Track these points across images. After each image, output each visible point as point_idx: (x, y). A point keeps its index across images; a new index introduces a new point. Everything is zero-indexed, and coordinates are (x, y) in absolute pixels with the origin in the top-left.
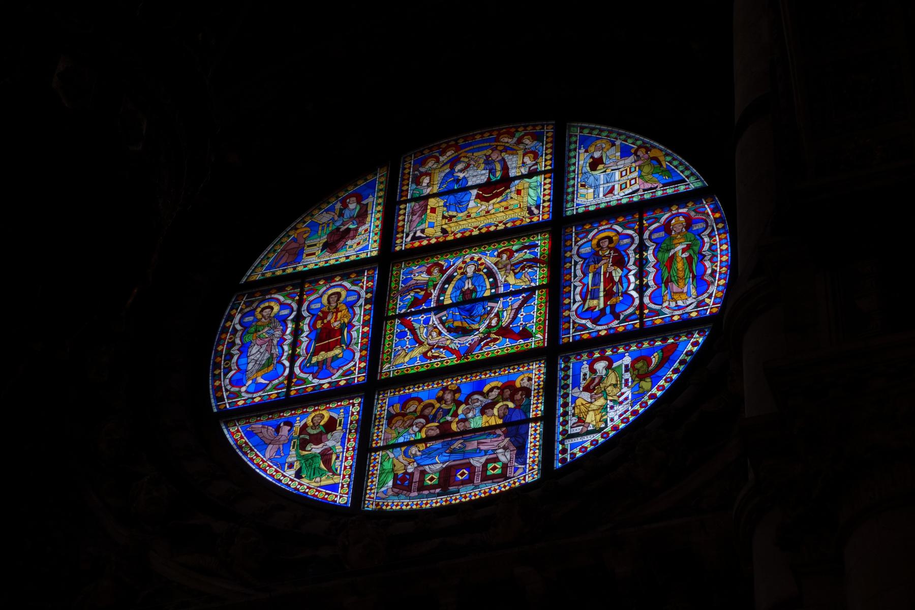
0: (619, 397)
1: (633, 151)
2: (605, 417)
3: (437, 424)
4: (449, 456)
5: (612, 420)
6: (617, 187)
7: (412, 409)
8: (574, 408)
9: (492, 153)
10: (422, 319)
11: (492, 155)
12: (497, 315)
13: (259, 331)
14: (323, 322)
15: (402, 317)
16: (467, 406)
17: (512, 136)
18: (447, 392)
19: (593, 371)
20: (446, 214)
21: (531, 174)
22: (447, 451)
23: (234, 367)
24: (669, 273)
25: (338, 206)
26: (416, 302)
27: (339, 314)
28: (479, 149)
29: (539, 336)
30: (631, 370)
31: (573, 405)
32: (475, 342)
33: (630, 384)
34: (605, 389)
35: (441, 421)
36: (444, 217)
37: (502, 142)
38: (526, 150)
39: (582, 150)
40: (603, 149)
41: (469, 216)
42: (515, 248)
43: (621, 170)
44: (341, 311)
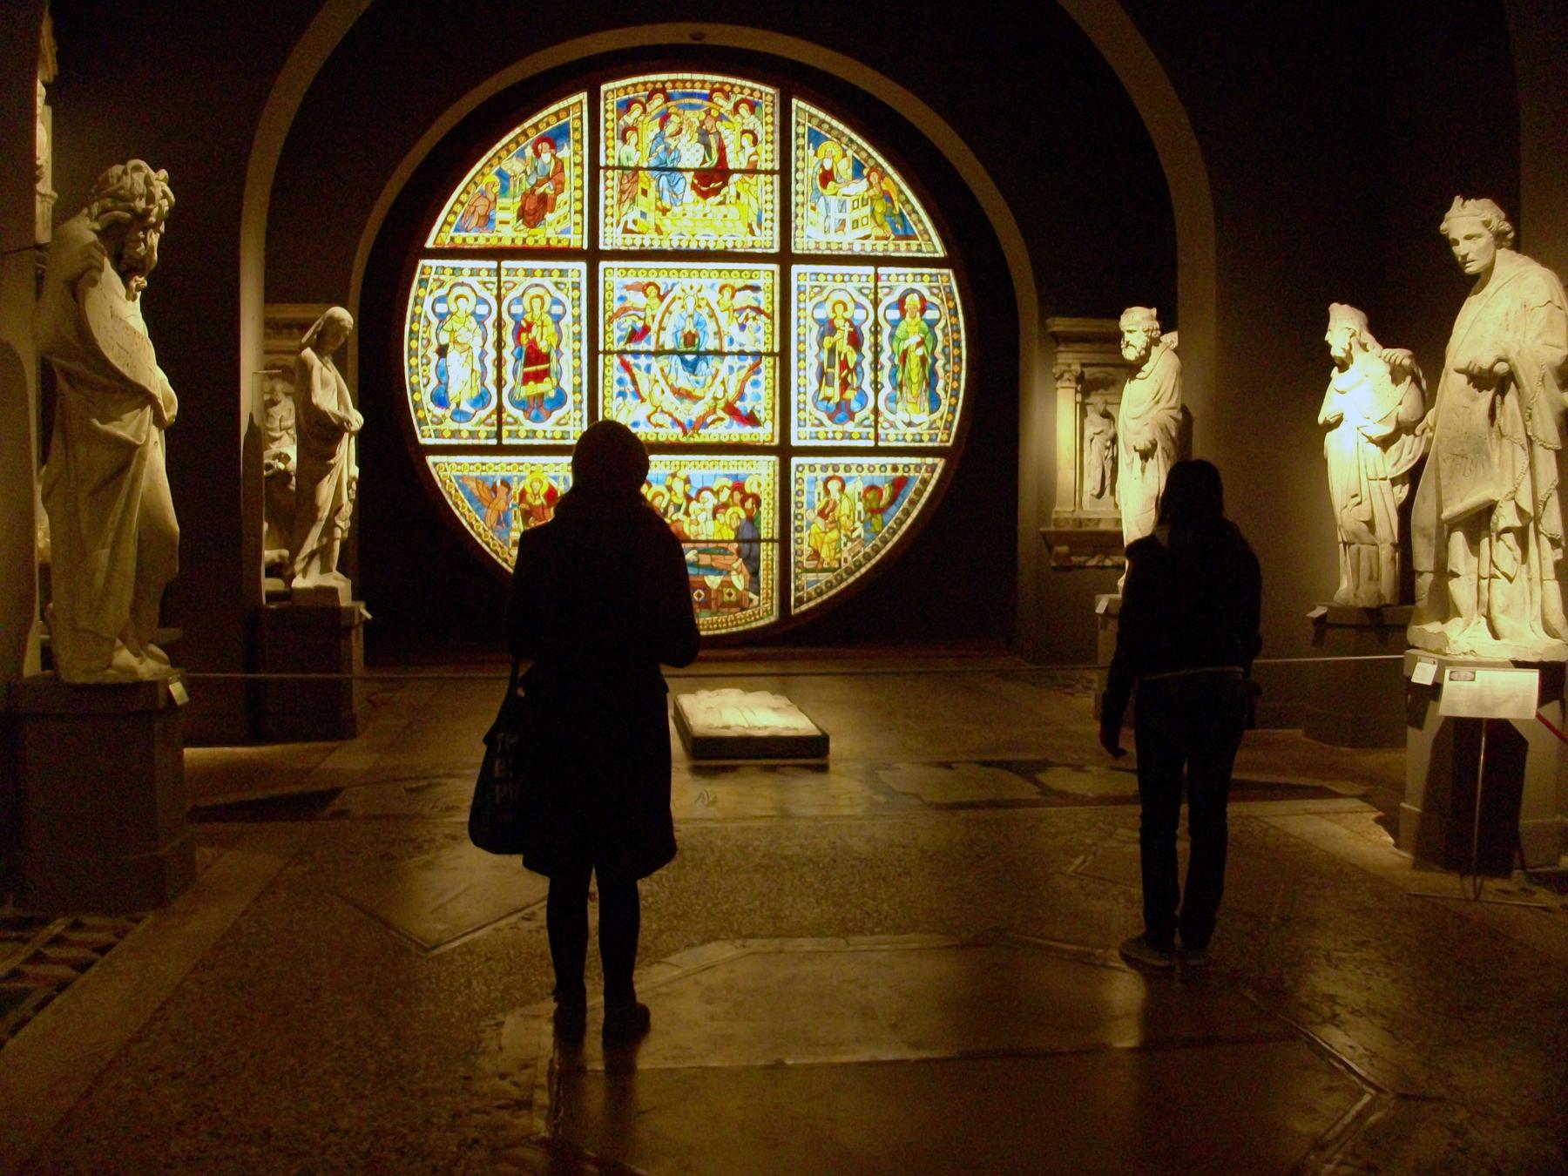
2: (838, 556)
5: (846, 561)
6: (849, 224)
12: (723, 382)
14: (527, 337)
15: (621, 353)
17: (727, 98)
19: (827, 492)
20: (659, 204)
21: (752, 171)
23: (433, 375)
24: (903, 372)
25: (529, 152)
26: (636, 335)
28: (692, 107)
29: (768, 425)
33: (862, 518)
36: (657, 208)
38: (746, 128)
39: (811, 152)
40: (833, 157)
42: (739, 283)
43: (853, 198)
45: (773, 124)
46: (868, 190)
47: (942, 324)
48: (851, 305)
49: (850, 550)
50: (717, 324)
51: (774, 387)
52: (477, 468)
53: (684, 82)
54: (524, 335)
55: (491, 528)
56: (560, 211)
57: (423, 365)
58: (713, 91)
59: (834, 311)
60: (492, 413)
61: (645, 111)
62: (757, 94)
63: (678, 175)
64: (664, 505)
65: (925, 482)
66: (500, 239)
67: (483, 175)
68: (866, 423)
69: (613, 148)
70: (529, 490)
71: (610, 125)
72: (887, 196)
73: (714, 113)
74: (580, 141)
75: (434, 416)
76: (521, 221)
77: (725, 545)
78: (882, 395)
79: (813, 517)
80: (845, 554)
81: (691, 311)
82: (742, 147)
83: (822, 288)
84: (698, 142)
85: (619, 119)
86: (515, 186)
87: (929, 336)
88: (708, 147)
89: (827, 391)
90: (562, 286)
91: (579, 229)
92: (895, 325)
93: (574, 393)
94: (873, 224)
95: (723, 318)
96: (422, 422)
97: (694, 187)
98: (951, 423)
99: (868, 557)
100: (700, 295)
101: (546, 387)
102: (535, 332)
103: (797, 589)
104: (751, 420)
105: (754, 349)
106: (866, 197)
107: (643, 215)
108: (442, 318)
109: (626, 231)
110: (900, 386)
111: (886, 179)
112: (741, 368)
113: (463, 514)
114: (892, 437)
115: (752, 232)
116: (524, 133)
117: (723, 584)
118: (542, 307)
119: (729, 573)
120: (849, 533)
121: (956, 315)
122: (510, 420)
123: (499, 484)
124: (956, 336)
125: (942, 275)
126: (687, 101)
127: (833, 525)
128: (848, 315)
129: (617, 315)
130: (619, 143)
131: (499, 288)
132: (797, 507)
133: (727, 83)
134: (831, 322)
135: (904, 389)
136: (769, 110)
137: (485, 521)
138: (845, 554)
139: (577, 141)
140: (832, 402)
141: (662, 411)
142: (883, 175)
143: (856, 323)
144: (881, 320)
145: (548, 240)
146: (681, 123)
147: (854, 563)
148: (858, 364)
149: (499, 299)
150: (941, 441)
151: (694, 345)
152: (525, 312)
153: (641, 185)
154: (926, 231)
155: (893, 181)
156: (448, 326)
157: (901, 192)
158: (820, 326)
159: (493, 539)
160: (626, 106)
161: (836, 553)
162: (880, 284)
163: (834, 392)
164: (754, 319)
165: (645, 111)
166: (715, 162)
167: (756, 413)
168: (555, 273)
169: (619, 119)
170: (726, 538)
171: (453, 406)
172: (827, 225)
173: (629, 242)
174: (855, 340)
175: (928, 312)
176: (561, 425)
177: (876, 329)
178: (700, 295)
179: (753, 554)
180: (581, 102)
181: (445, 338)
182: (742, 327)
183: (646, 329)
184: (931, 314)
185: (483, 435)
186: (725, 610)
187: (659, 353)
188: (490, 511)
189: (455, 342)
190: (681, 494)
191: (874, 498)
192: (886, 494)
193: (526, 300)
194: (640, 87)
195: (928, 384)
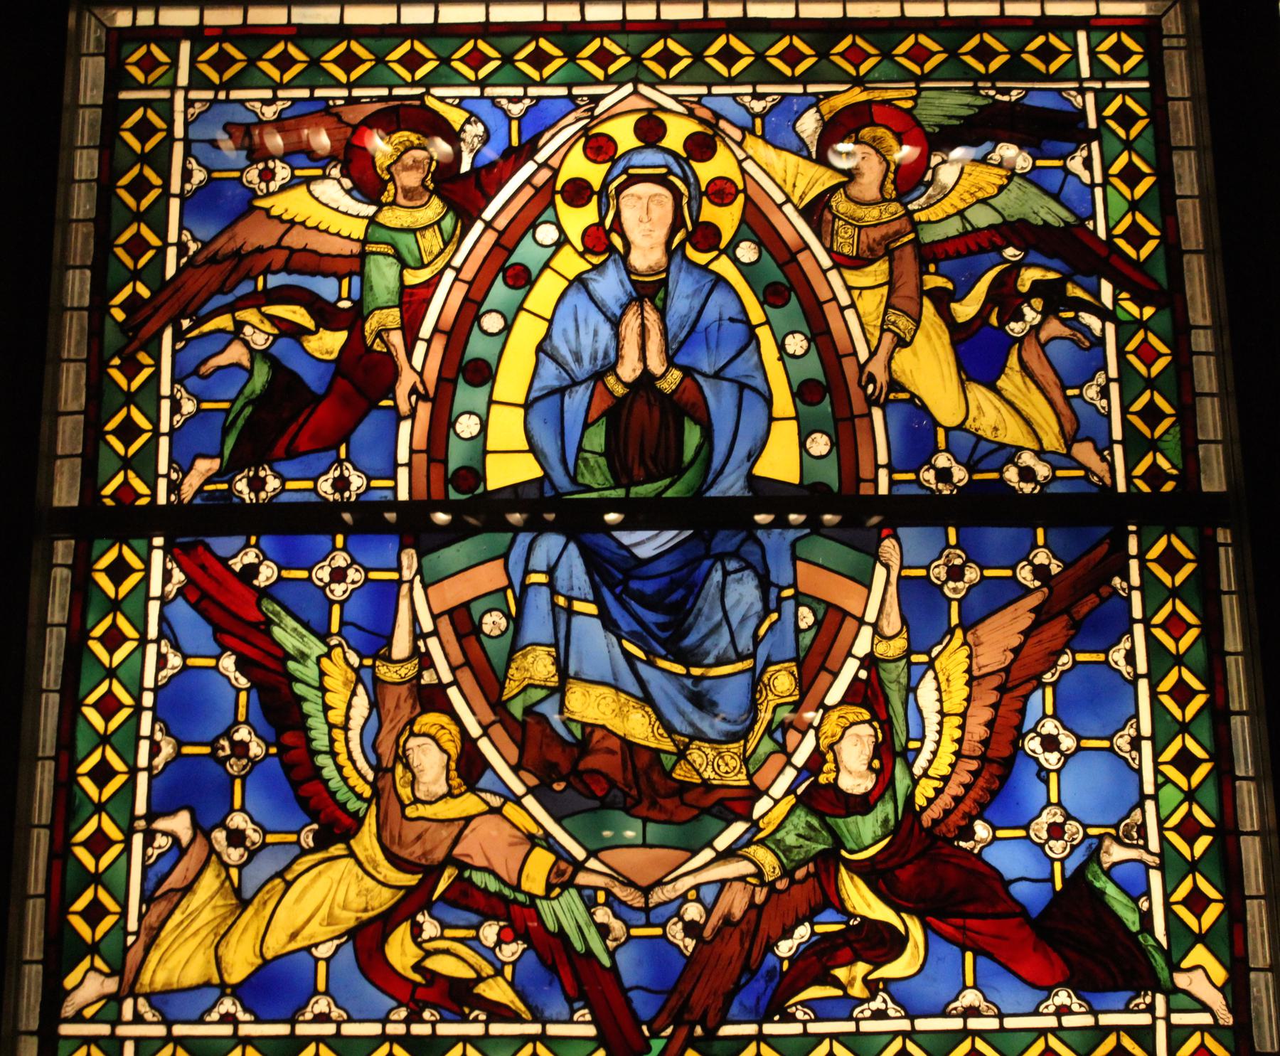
10: (338, 590)
32: (727, 920)
50: (819, 333)
100: (706, 171)
151: (676, 470)
164: (1052, 297)
178: (706, 171)
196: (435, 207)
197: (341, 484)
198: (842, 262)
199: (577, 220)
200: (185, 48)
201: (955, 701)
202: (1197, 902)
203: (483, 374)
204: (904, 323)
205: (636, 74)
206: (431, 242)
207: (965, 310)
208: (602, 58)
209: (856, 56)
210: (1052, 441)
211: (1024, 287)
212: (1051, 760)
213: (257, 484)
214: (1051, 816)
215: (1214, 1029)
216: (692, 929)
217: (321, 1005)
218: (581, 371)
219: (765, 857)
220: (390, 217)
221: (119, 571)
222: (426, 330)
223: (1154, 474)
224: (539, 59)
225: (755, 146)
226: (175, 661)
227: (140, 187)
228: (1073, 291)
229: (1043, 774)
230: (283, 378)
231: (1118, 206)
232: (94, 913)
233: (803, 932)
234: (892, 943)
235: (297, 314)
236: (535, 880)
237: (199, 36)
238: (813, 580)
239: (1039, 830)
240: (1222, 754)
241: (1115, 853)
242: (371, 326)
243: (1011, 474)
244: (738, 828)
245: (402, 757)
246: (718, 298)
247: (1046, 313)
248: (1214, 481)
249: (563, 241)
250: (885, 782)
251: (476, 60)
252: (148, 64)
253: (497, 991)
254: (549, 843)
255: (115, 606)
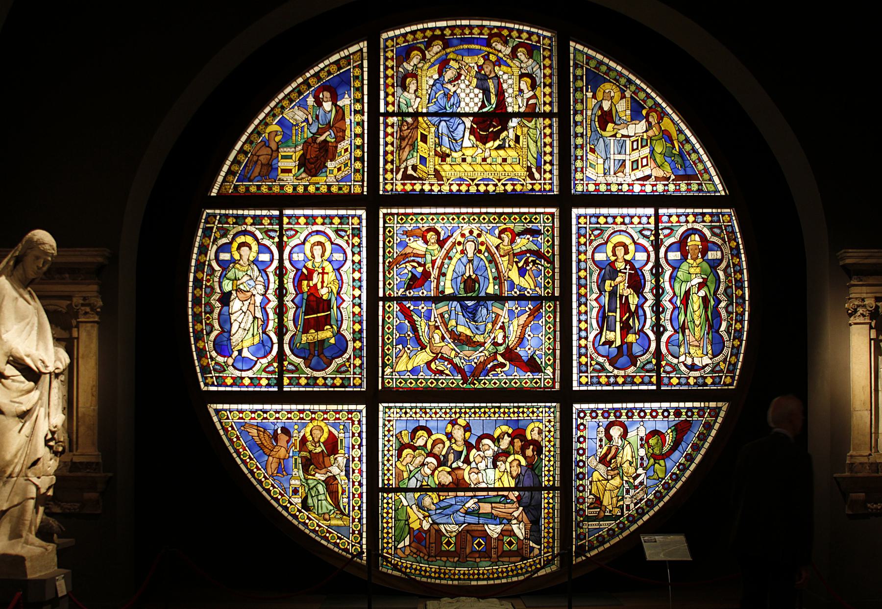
0: (635, 479)
1: (644, 112)
2: (621, 503)
3: (449, 470)
4: (464, 517)
5: (628, 507)
6: (628, 164)
7: (420, 442)
8: (591, 483)
9: (484, 63)
10: (423, 311)
11: (484, 66)
13: (239, 279)
14: (308, 285)
15: (400, 300)
16: (480, 453)
17: (506, 43)
18: (457, 427)
19: (609, 438)
20: (438, 149)
21: (530, 114)
22: (462, 510)
23: (217, 326)
25: (311, 101)
26: (415, 282)
27: (325, 276)
28: (471, 53)
30: (646, 446)
31: (590, 479)
34: (621, 466)
35: (454, 465)
36: (436, 154)
37: (495, 49)
38: (523, 71)
40: (612, 98)
41: (464, 160)
42: (519, 228)
43: (633, 139)
44: (328, 273)
45: (551, 67)
46: (646, 131)
47: (724, 265)
48: (632, 248)
49: (632, 497)
50: (497, 268)
51: (555, 331)
52: (259, 415)
53: (462, 27)
54: (305, 283)
55: (272, 476)
56: (340, 160)
57: (206, 314)
58: (491, 36)
59: (614, 254)
60: (274, 360)
61: (424, 58)
62: (534, 38)
63: (458, 120)
64: (444, 453)
65: (708, 426)
66: (282, 187)
67: (267, 125)
68: (648, 367)
69: (393, 95)
70: (310, 438)
71: (390, 72)
72: (666, 136)
73: (493, 58)
74: (360, 89)
75: (217, 363)
76: (302, 170)
77: (506, 493)
78: (664, 339)
79: (595, 464)
80: (627, 501)
81: (470, 255)
82: (521, 91)
83: (602, 231)
84: (477, 87)
85: (398, 67)
86: (297, 135)
87: (711, 277)
88: (486, 92)
89: (610, 336)
90: (343, 234)
91: (358, 177)
92: (675, 268)
93: (354, 340)
94: (653, 165)
95: (504, 262)
96: (205, 370)
97: (472, 131)
98: (735, 364)
99: (650, 504)
100: (480, 240)
101: (326, 334)
102: (316, 279)
103: (578, 536)
104: (532, 365)
105: (534, 294)
106: (645, 137)
107: (423, 160)
108: (225, 266)
109: (406, 177)
110: (683, 328)
111: (666, 120)
112: (523, 312)
113: (244, 462)
114: (675, 381)
115: (531, 176)
116: (306, 82)
117: (503, 533)
118: (322, 255)
119: (509, 521)
120: (632, 481)
121: (738, 255)
122: (291, 367)
123: (279, 431)
124: (739, 276)
125: (723, 216)
126: (465, 46)
127: (616, 472)
128: (628, 257)
129: (396, 262)
130: (399, 90)
131: (281, 237)
132: (578, 453)
133: (505, 28)
134: (612, 264)
135: (687, 331)
136: (547, 54)
137: (265, 469)
138: (627, 501)
139: (357, 89)
140: (614, 346)
141: (442, 358)
142: (662, 114)
143: (637, 266)
144: (663, 261)
145: (329, 187)
146: (459, 68)
147: (637, 510)
148: (640, 306)
149: (281, 247)
150: (725, 384)
151: (474, 291)
152: (306, 260)
153: (420, 131)
154: (706, 170)
155: (672, 120)
156: (230, 275)
157: (680, 131)
158: (601, 269)
159: (274, 487)
160: (404, 55)
161: (618, 501)
162: (661, 226)
163: (615, 336)
164: (534, 262)
165: (424, 58)
166: (494, 106)
167: (537, 359)
168: (336, 221)
169: (398, 67)
170: (506, 485)
171: (236, 353)
172: (606, 166)
173: (408, 188)
174: (636, 284)
175: (709, 253)
176: (341, 373)
177: (657, 270)
178: (480, 240)
179: (533, 503)
180: (361, 50)
181: (228, 286)
182: (522, 272)
183: (426, 275)
184: (711, 255)
185: (264, 382)
186: (507, 559)
187: (440, 298)
188: (271, 458)
189: (238, 290)
190: (461, 442)
191: (657, 443)
192: (669, 439)
193: (308, 246)
194: (419, 35)
195: (711, 327)
196: (437, 245)
197: (423, 293)
198: (501, 256)
199: (460, 248)
200: (396, 216)
201: (515, 329)
202: (549, 360)
203: (444, 275)
204: (511, 267)
205: (469, 222)
206: (436, 252)
207: (520, 265)
208: (464, 219)
209: (505, 219)
210: (533, 287)
211: (530, 261)
212: (529, 338)
213: (410, 293)
214: (529, 347)
215: (550, 378)
216: (475, 363)
217: (421, 373)
218: (460, 274)
219: (486, 353)
220: (429, 247)
221: (389, 307)
222: (435, 267)
223: (548, 293)
224: (453, 219)
225: (488, 235)
226: (398, 322)
227: (389, 242)
228: (537, 261)
229: (528, 340)
230: (413, 275)
231: (546, 246)
232: (388, 360)
233: (491, 364)
234: (505, 365)
235: (415, 264)
236: (452, 356)
237: (398, 214)
238: (494, 309)
239: (527, 349)
240: (555, 338)
241: (537, 352)
242: (427, 267)
243: (526, 293)
244: (483, 348)
245: (433, 337)
246: (482, 262)
247: (533, 265)
248: (557, 294)
249: (457, 252)
250: (504, 341)
251: (443, 219)
252: (390, 220)
253: (447, 372)
254: (454, 349)
255: (389, 312)
